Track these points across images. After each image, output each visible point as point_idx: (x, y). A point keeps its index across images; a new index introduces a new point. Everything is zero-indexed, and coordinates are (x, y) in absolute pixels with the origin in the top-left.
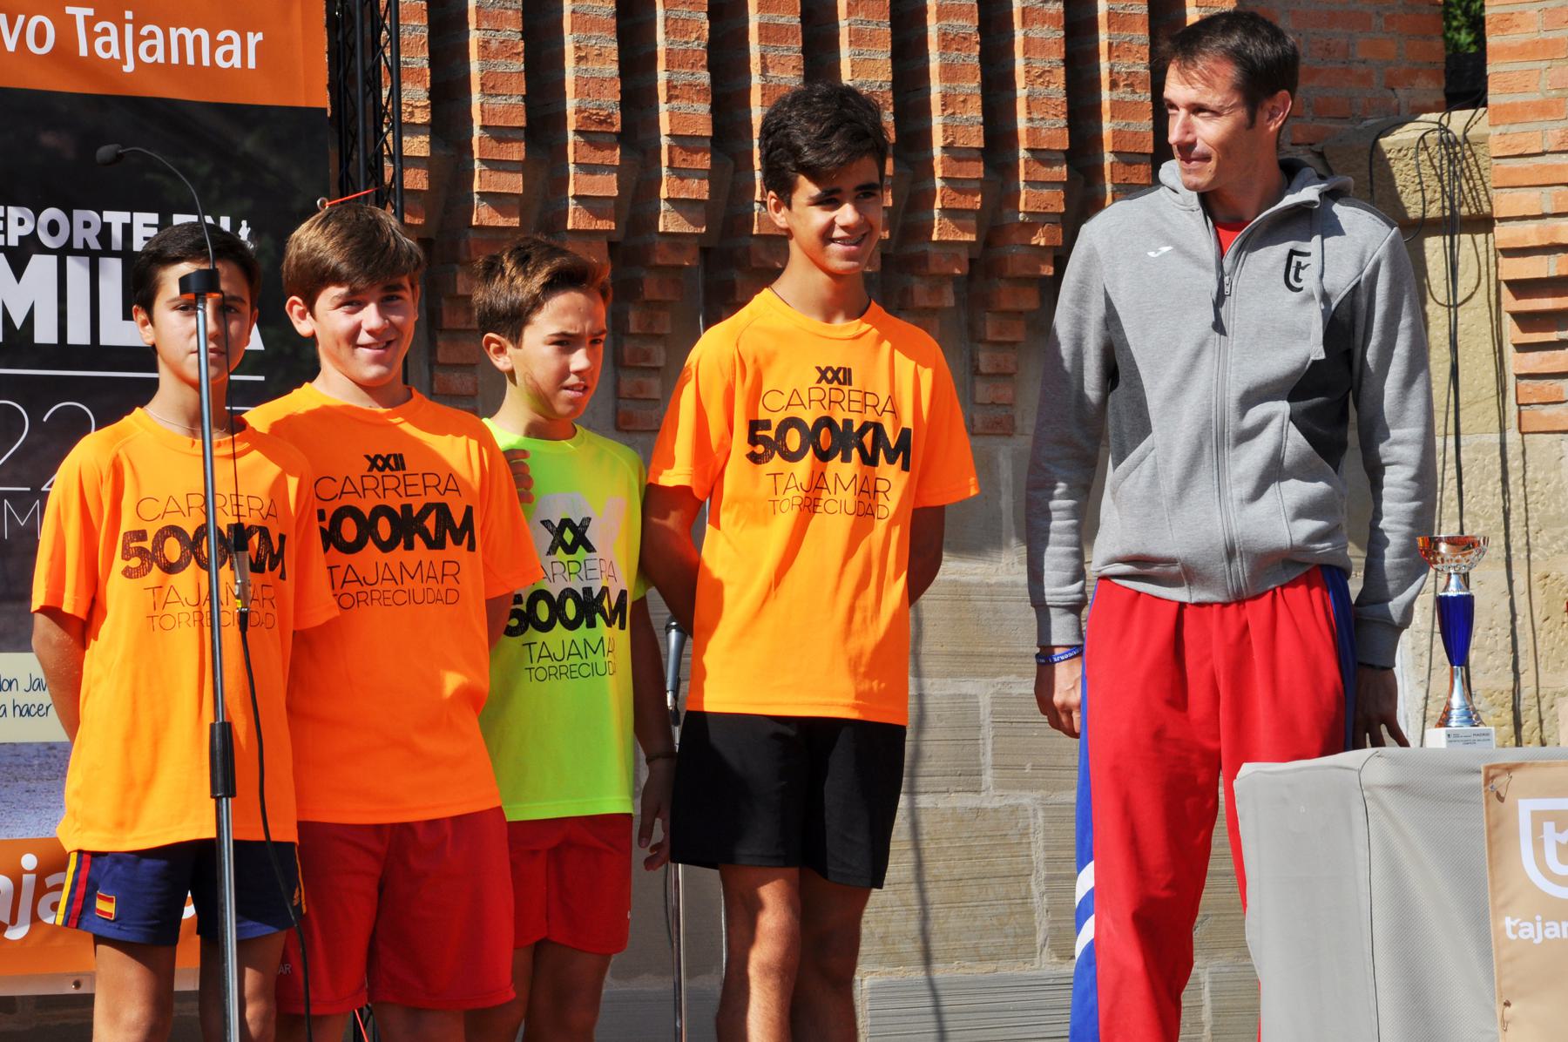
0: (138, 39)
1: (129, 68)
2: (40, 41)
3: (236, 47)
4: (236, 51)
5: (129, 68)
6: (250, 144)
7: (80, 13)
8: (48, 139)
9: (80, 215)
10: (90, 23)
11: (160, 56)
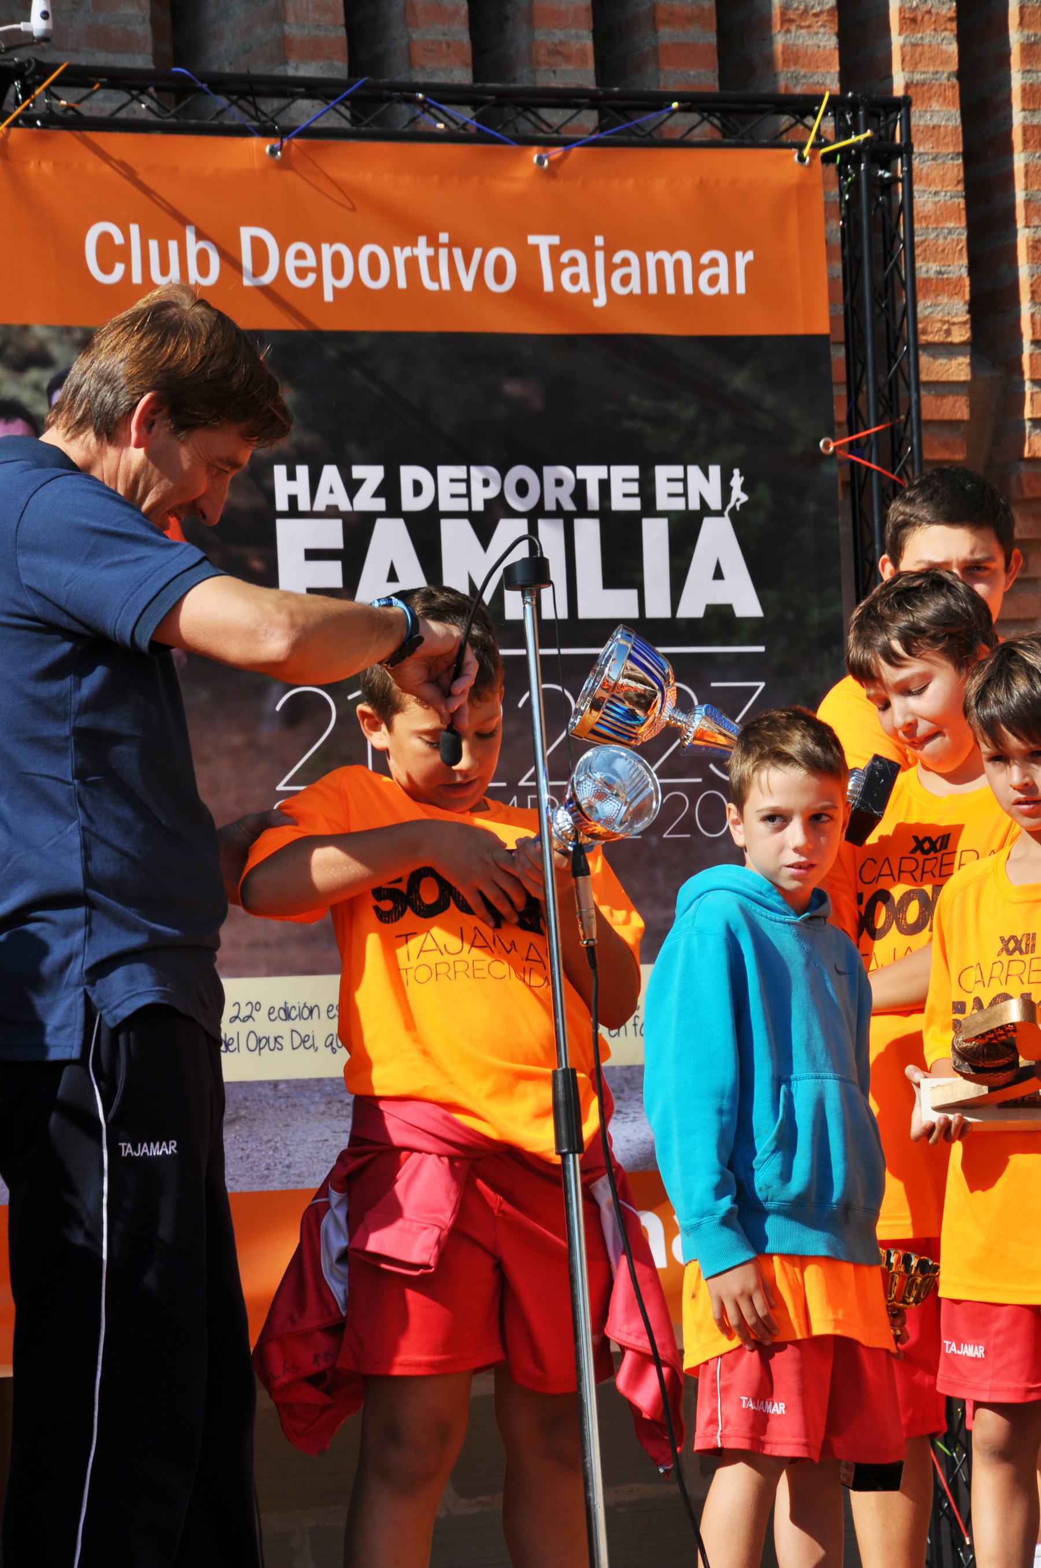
2: (500, 275)
4: (721, 276)
5: (600, 301)
6: (740, 380)
7: (543, 242)
8: (513, 388)
9: (551, 472)
10: (555, 252)
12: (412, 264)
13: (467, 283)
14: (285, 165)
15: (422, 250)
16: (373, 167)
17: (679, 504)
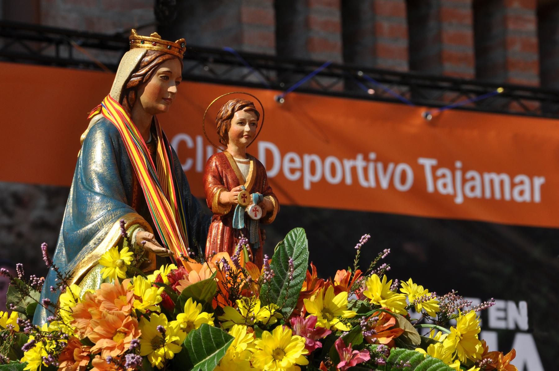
0: (464, 181)
1: (459, 200)
2: (403, 180)
3: (527, 187)
5: (459, 200)
6: (537, 252)
7: (427, 163)
10: (434, 169)
11: (478, 193)
12: (354, 170)
13: (384, 184)
14: (286, 107)
15: (360, 163)
16: (337, 114)
17: (501, 325)
